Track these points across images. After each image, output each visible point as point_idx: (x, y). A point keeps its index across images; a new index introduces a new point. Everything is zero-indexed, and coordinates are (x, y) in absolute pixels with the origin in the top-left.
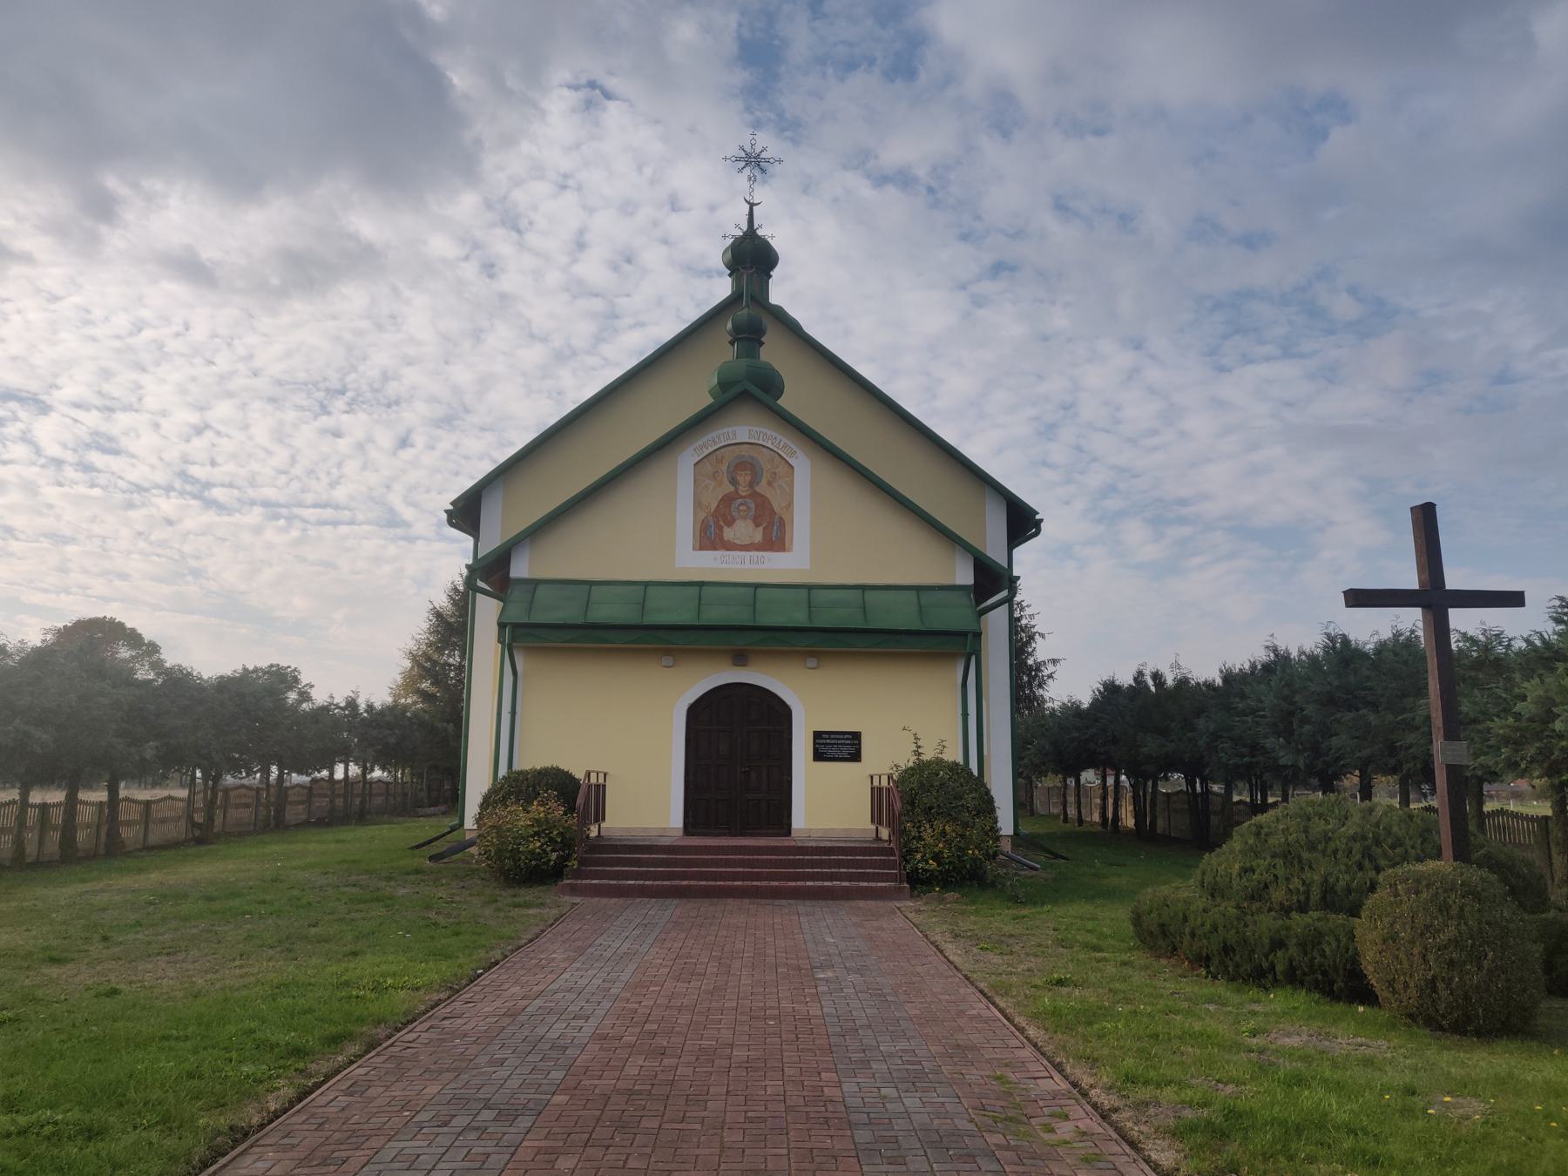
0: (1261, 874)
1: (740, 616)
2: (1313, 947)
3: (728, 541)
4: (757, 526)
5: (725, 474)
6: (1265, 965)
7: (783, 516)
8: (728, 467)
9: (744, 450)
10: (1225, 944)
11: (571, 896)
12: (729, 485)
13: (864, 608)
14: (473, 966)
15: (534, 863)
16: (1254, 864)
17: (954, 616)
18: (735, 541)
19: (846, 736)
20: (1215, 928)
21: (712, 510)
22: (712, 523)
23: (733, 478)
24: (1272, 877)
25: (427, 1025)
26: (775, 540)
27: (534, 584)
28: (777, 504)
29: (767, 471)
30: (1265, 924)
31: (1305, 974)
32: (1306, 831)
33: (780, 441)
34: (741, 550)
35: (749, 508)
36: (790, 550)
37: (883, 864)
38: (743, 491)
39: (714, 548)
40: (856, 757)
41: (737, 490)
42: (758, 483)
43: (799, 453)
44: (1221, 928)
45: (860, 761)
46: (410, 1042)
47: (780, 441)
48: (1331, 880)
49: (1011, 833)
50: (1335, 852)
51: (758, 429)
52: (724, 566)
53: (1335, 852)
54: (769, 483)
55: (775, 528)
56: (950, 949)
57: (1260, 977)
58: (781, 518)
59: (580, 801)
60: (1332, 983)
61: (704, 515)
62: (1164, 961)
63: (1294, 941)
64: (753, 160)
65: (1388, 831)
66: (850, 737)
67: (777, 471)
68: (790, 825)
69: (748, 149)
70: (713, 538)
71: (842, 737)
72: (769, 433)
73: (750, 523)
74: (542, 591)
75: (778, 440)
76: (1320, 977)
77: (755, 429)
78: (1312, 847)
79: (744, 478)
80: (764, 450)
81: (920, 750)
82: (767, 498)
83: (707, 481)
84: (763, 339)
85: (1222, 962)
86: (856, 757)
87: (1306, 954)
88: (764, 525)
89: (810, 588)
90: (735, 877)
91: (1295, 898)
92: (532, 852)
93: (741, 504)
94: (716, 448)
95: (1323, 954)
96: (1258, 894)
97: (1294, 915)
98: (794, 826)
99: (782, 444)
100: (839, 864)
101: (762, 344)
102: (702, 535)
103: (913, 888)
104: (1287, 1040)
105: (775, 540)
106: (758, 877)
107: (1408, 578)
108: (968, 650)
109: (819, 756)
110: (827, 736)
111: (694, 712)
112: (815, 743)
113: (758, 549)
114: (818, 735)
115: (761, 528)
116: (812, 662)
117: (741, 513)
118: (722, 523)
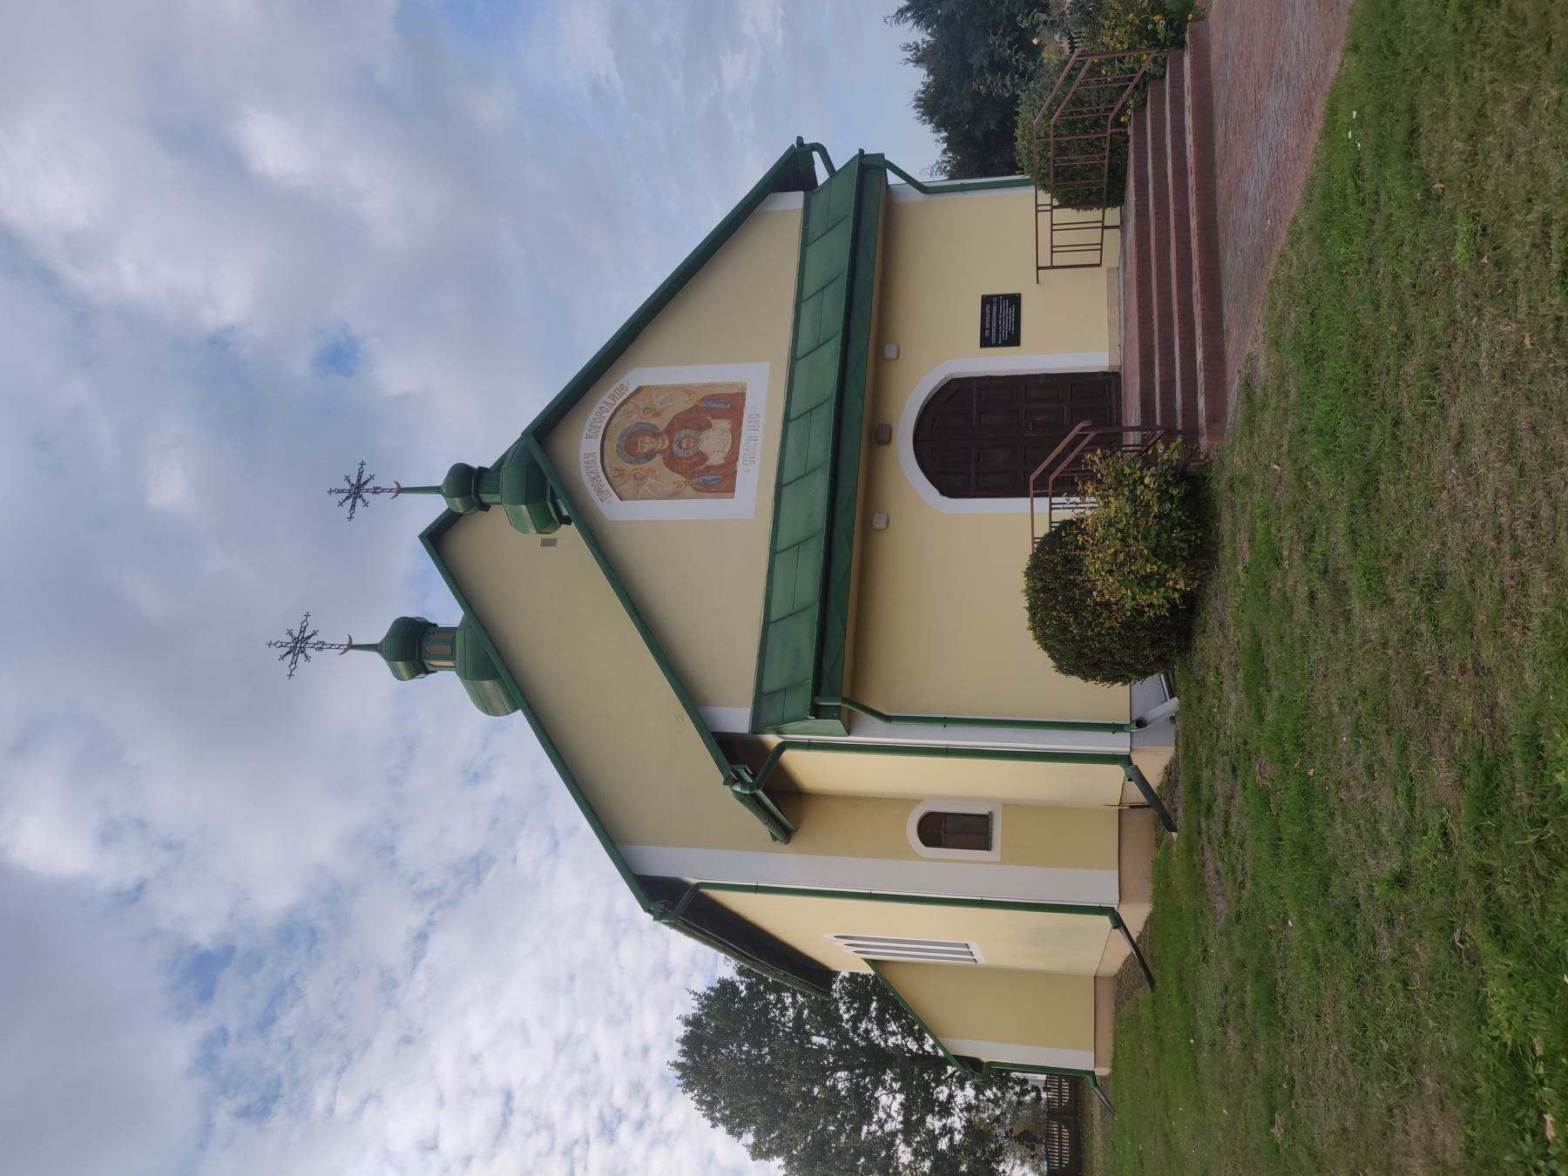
3: (725, 459)
4: (709, 426)
5: (639, 466)
8: (630, 463)
21: (684, 479)
22: (700, 480)
23: (646, 457)
26: (731, 405)
28: (683, 404)
29: (641, 417)
34: (739, 444)
35: (687, 437)
36: (744, 387)
39: (735, 473)
40: (1014, 300)
41: (660, 452)
42: (656, 427)
43: (624, 380)
45: (1020, 295)
51: (587, 426)
52: (757, 460)
54: (657, 415)
55: (714, 405)
58: (702, 400)
66: (988, 307)
67: (642, 407)
70: (720, 477)
71: (988, 316)
72: (593, 415)
75: (605, 405)
77: (586, 431)
79: (647, 444)
80: (614, 422)
82: (674, 417)
83: (646, 487)
86: (1014, 300)
88: (709, 418)
93: (680, 446)
102: (714, 490)
105: (731, 405)
109: (1013, 340)
110: (987, 332)
112: (997, 345)
113: (740, 424)
114: (985, 342)
115: (713, 421)
117: (692, 444)
118: (702, 468)
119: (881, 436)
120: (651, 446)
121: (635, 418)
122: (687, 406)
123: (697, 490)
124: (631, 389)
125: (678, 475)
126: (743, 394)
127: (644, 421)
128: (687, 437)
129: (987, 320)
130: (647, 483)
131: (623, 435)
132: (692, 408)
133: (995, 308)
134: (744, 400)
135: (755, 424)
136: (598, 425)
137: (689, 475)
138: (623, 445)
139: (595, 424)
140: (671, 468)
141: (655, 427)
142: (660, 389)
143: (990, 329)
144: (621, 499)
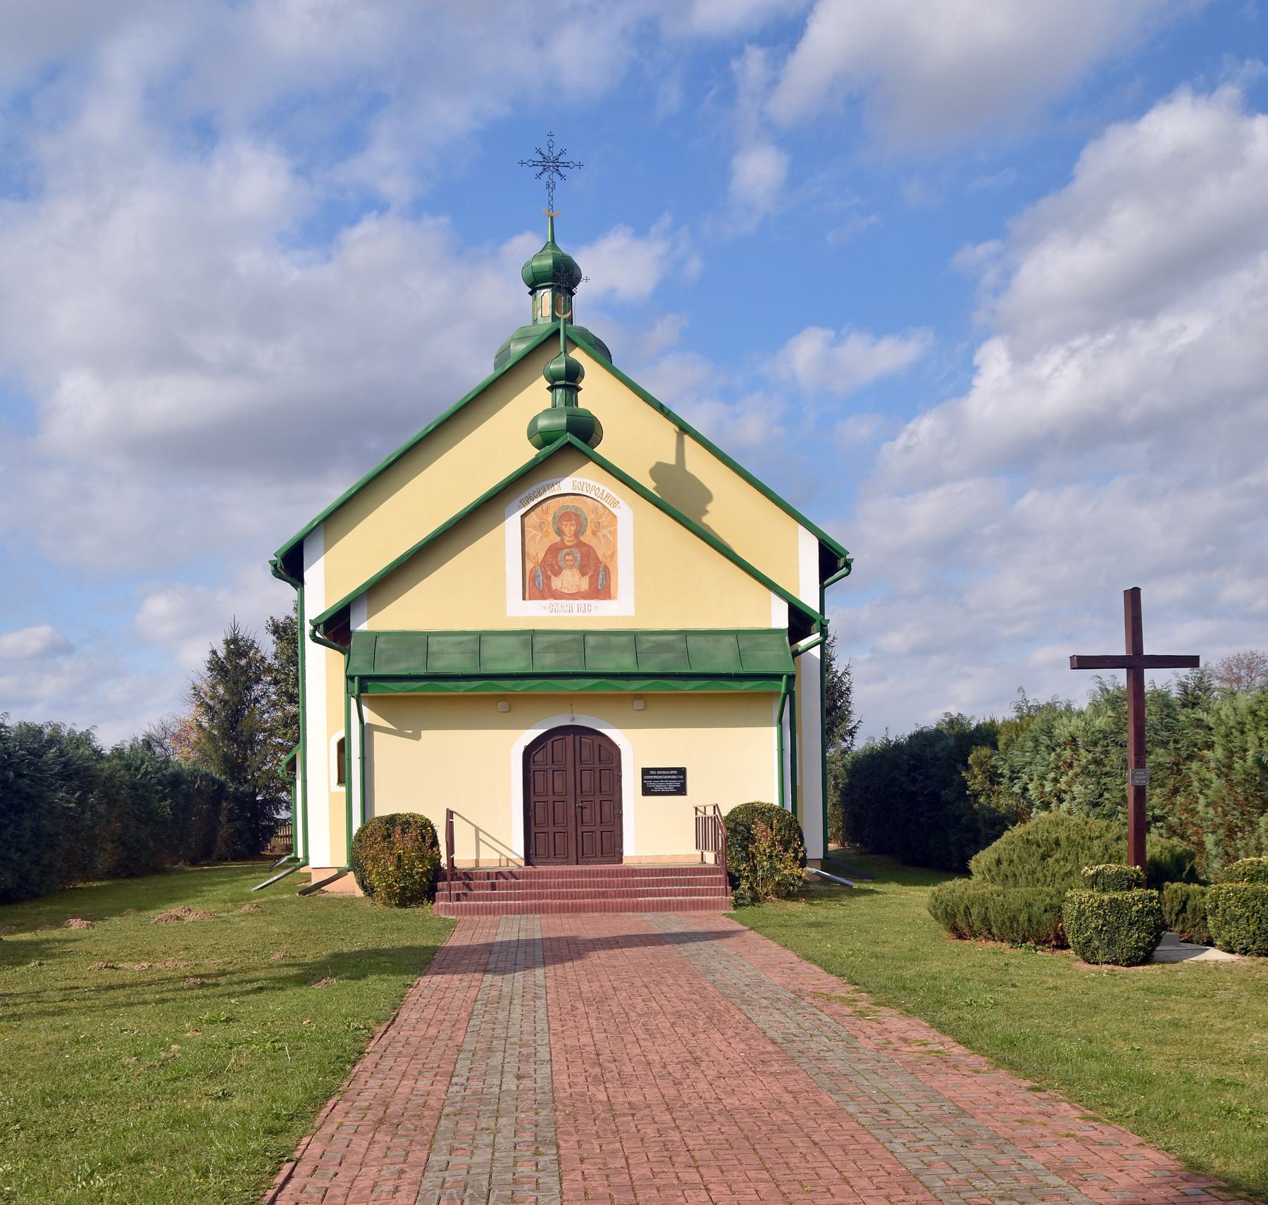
4: (583, 574)
8: (554, 518)
17: (773, 659)
19: (672, 772)
23: (558, 529)
26: (601, 588)
29: (591, 522)
34: (568, 599)
35: (574, 557)
36: (615, 598)
39: (544, 598)
40: (681, 790)
41: (562, 540)
43: (622, 503)
45: (685, 794)
49: (822, 857)
52: (554, 614)
54: (594, 533)
55: (601, 576)
58: (606, 567)
66: (676, 772)
68: (622, 854)
72: (592, 483)
75: (601, 491)
83: (534, 532)
86: (681, 790)
98: (625, 854)
101: (579, 389)
105: (601, 588)
109: (647, 791)
110: (654, 772)
112: (643, 779)
113: (584, 598)
114: (646, 771)
117: (568, 563)
118: (549, 573)
120: (567, 533)
121: (591, 517)
122: (600, 556)
124: (614, 510)
127: (589, 524)
129: (664, 772)
130: (537, 533)
131: (577, 508)
132: (598, 559)
134: (604, 599)
135: (583, 609)
136: (585, 489)
137: (543, 564)
139: (585, 487)
140: (549, 549)
142: (614, 533)
144: (522, 516)
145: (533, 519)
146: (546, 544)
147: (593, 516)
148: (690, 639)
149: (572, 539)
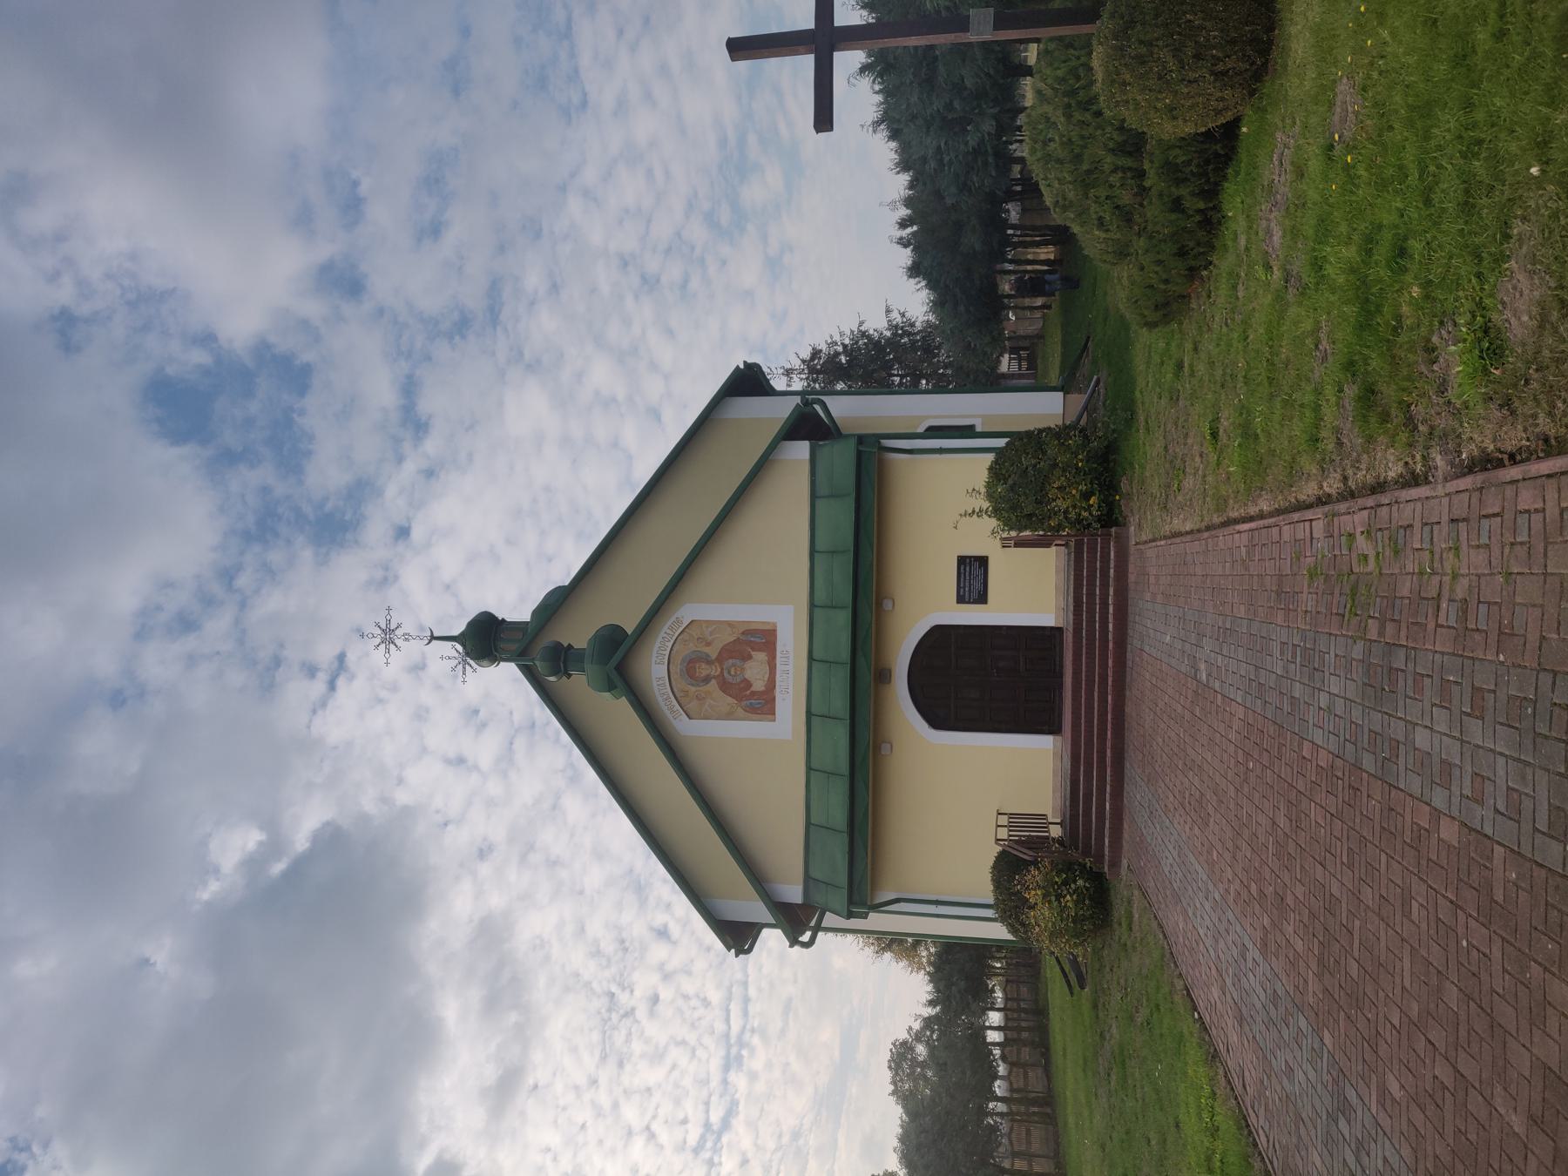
0: (1105, 212)
1: (841, 678)
2: (1181, 171)
3: (765, 686)
4: (750, 657)
5: (698, 688)
6: (1198, 218)
7: (741, 631)
8: (693, 685)
9: (675, 669)
10: (1175, 255)
11: (1120, 867)
12: (708, 685)
13: (833, 552)
14: (1190, 1020)
15: (1087, 902)
16: (1094, 216)
17: (840, 457)
18: (766, 679)
19: (962, 571)
20: (1159, 262)
22: (748, 702)
23: (703, 681)
24: (1108, 201)
25: (1250, 1111)
26: (765, 639)
27: (808, 880)
30: (1154, 211)
31: (1208, 181)
32: (1060, 161)
33: (666, 633)
34: (775, 673)
35: (734, 665)
37: (1092, 550)
38: (716, 671)
39: (774, 699)
40: (983, 561)
41: (714, 677)
43: (678, 614)
44: (1160, 257)
45: (987, 557)
46: (1268, 1141)
47: (666, 633)
48: (1111, 145)
50: (1082, 137)
51: (655, 654)
52: (791, 690)
53: (1082, 137)
54: (708, 644)
56: (1177, 524)
57: (1211, 222)
58: (743, 633)
59: (1026, 855)
60: (1217, 155)
61: (740, 710)
62: (1194, 305)
63: (1173, 189)
64: (388, 636)
65: (1063, 80)
66: (962, 568)
67: (696, 637)
68: (1052, 628)
69: (378, 640)
72: (657, 644)
73: (748, 664)
74: (815, 874)
75: (665, 635)
76: (1211, 167)
77: (654, 659)
78: (1078, 158)
79: (703, 670)
80: (675, 649)
81: (977, 510)
84: (566, 645)
85: (1195, 257)
86: (983, 561)
87: (1186, 180)
88: (750, 650)
89: (812, 606)
90: (1103, 701)
91: (1129, 181)
92: (1076, 903)
93: (729, 673)
94: (673, 698)
95: (1189, 163)
96: (1126, 216)
97: (1147, 183)
98: (1052, 624)
99: (668, 631)
100: (1091, 594)
103: (1117, 524)
104: (1275, 238)
105: (765, 639)
106: (1104, 679)
107: (805, 64)
108: (876, 450)
109: (982, 598)
110: (962, 590)
111: (938, 721)
112: (969, 602)
113: (774, 657)
114: (961, 599)
115: (753, 653)
116: (888, 605)
117: (738, 673)
118: (748, 692)
119: (883, 676)
120: (708, 672)
123: (746, 711)
125: (729, 698)
126: (775, 631)
128: (734, 665)
129: (962, 580)
132: (735, 640)
133: (968, 569)
136: (664, 652)
137: (739, 698)
138: (684, 669)
141: (708, 655)
143: (964, 588)
144: (690, 718)
145: (693, 706)
146: (718, 693)
147: (691, 645)
148: (818, 548)
149: (714, 667)
